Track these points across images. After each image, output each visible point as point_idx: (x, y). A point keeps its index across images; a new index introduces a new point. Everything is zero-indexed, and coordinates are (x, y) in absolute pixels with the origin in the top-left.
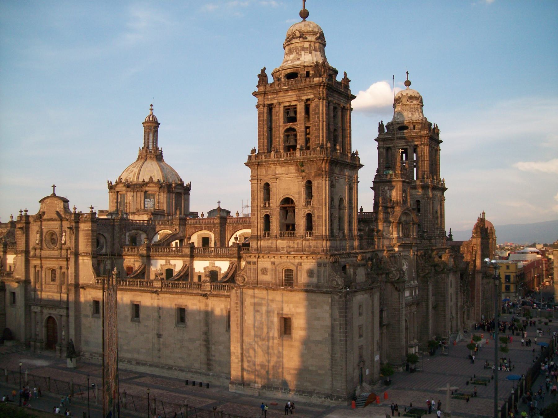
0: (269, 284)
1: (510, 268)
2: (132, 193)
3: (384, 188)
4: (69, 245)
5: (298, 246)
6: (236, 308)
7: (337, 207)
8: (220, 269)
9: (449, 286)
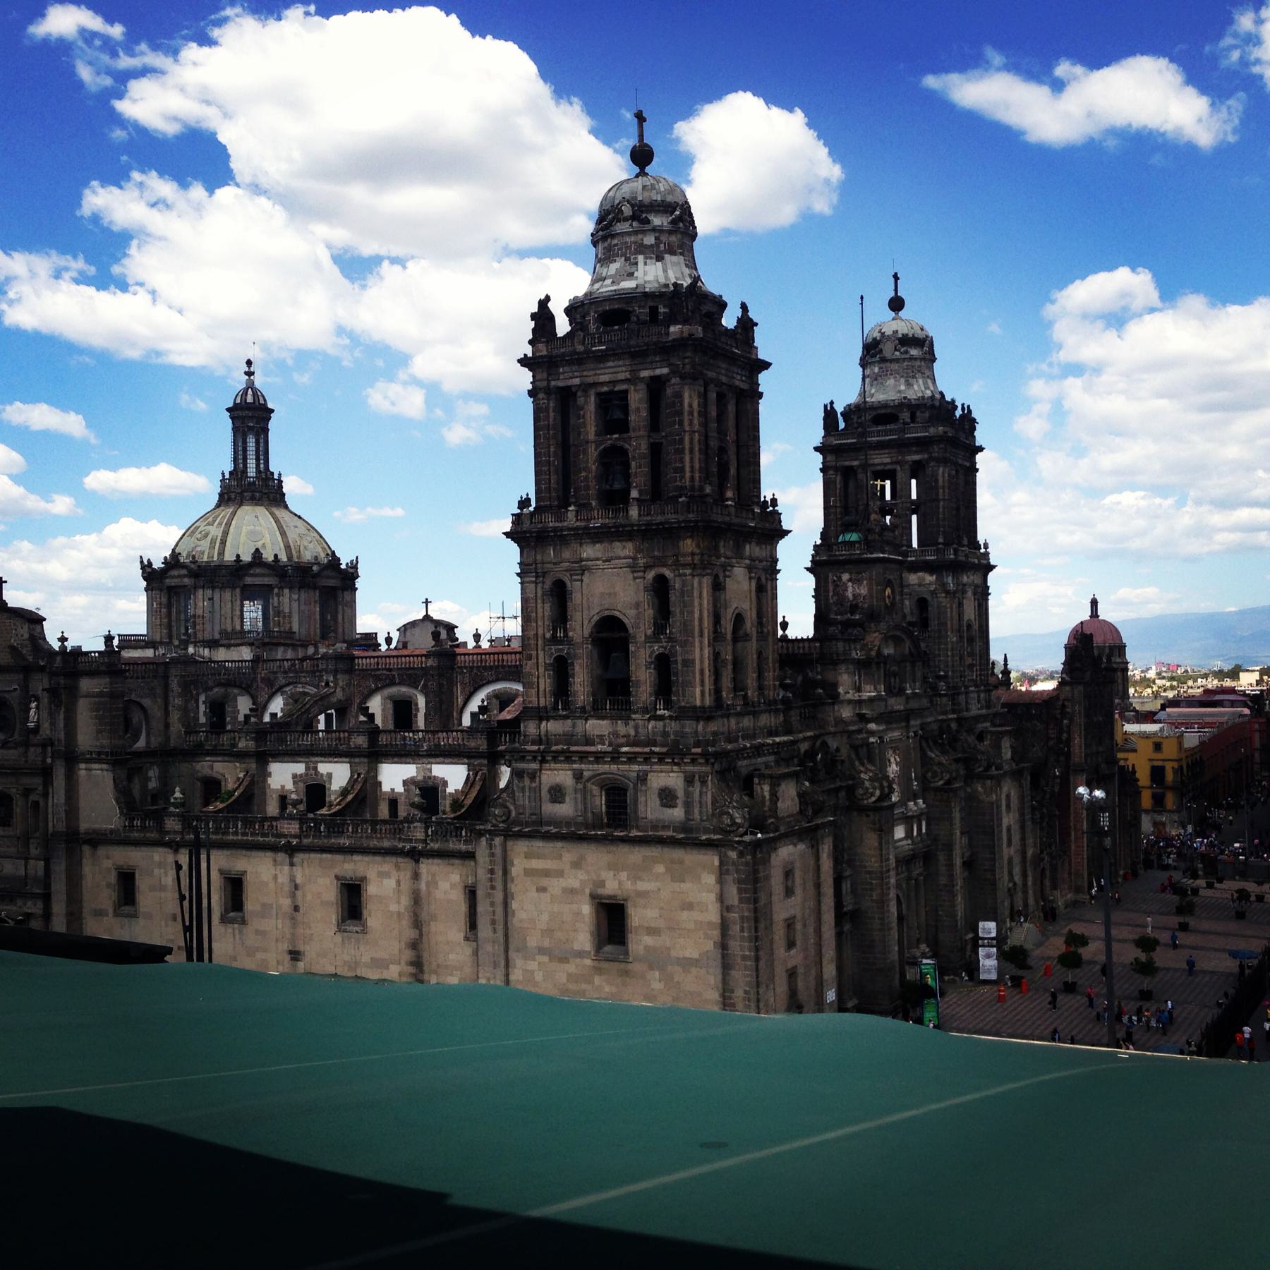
0: (568, 824)
1: (1164, 747)
2: (209, 593)
3: (840, 579)
4: (48, 732)
5: (637, 732)
6: (489, 884)
7: (729, 637)
8: (445, 783)
9: (1004, 807)
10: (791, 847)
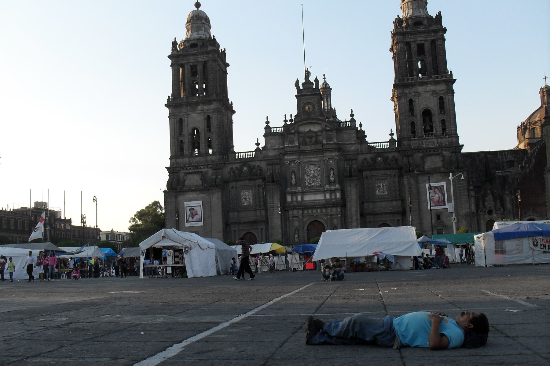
10: (195, 195)
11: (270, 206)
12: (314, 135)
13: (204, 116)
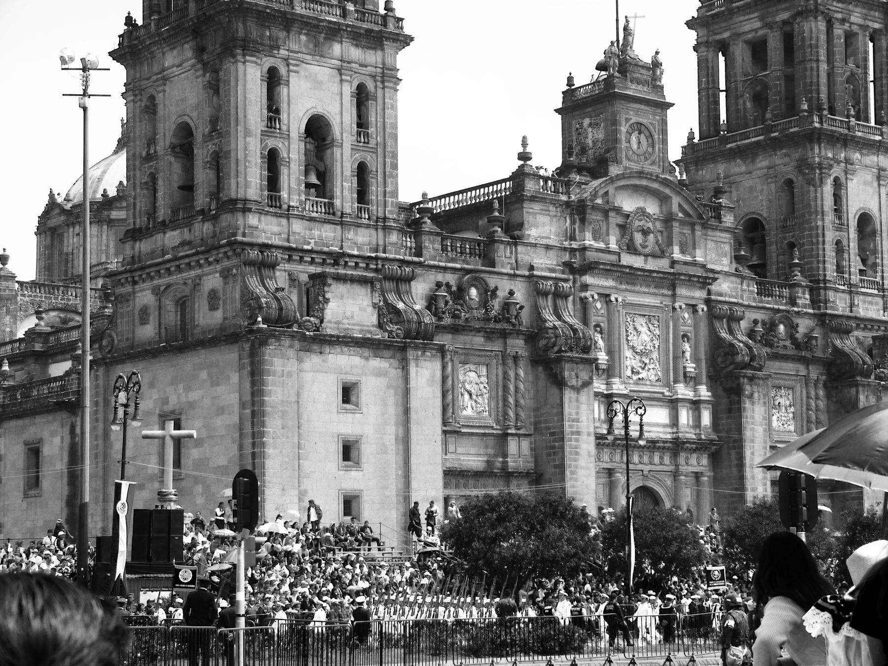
0: (150, 343)
10: (356, 360)
11: (571, 426)
12: (650, 225)
13: (351, 82)
